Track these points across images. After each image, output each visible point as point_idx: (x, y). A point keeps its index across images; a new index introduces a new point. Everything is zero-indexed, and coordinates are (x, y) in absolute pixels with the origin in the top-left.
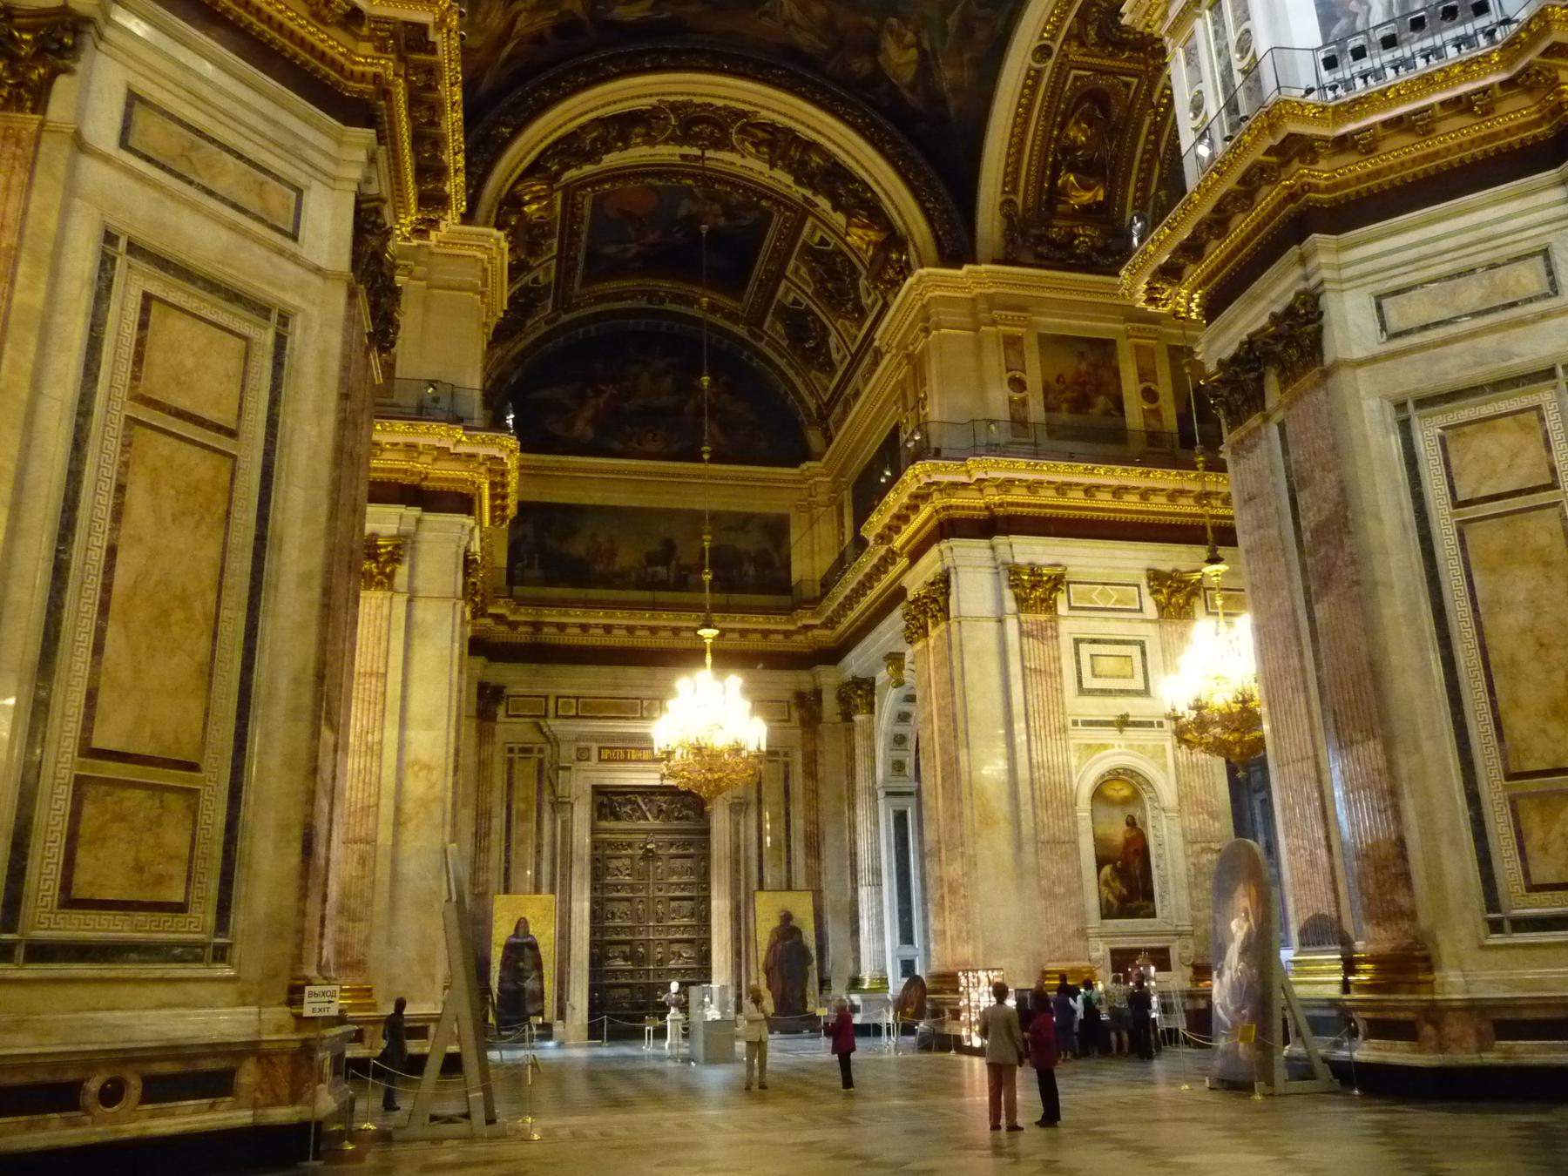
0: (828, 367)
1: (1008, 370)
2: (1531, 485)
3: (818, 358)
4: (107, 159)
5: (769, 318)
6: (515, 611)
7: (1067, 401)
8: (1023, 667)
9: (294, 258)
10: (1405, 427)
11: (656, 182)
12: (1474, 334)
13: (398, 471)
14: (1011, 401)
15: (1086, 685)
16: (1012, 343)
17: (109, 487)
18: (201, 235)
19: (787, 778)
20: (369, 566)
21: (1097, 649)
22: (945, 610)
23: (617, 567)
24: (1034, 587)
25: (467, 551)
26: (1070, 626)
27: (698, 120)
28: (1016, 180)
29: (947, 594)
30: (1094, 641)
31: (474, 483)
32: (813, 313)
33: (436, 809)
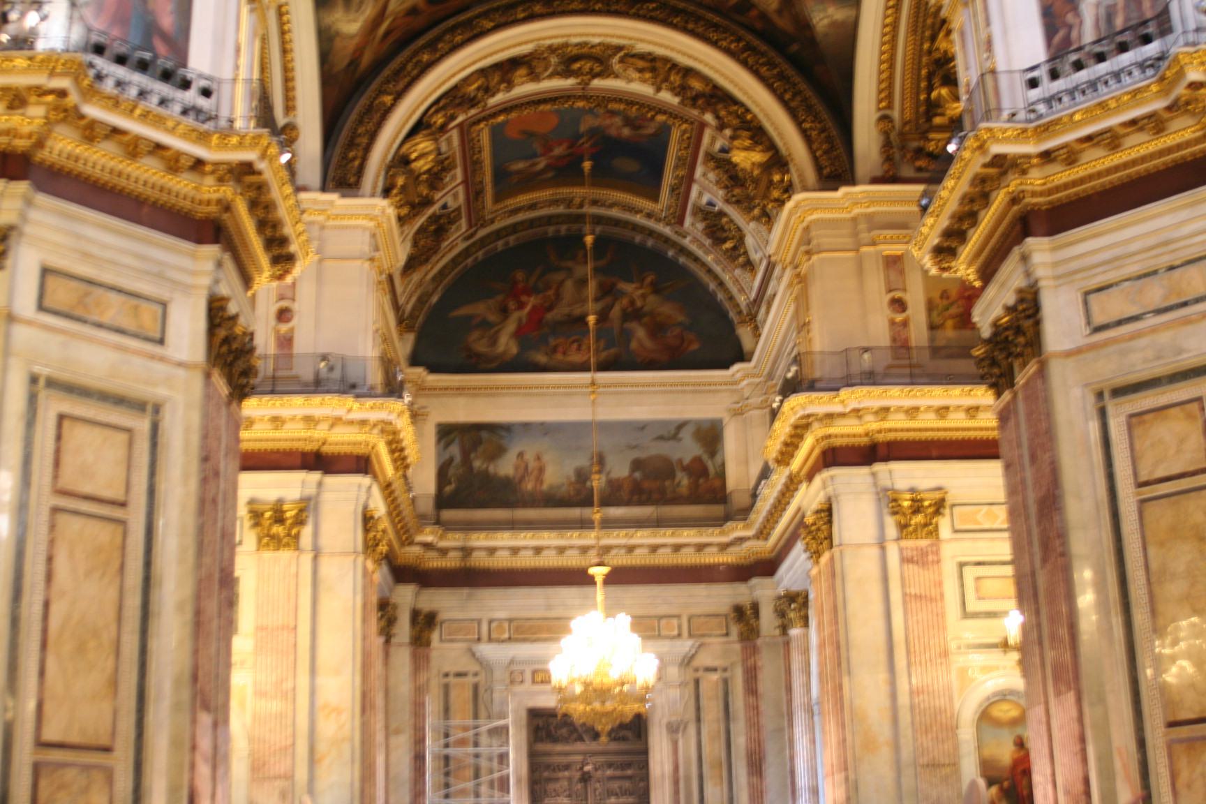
0: (749, 265)
2: (1192, 468)
3: (738, 255)
4: (29, 323)
6: (441, 538)
7: (953, 317)
8: (904, 595)
9: (162, 359)
10: (1103, 413)
11: (547, 107)
12: (1154, 330)
14: (892, 323)
17: (42, 559)
18: (95, 359)
19: (726, 694)
20: (278, 529)
22: (830, 537)
23: (545, 487)
24: (916, 511)
25: (365, 508)
27: (576, 58)
28: (890, 97)
29: (830, 522)
30: (979, 564)
33: (346, 748)
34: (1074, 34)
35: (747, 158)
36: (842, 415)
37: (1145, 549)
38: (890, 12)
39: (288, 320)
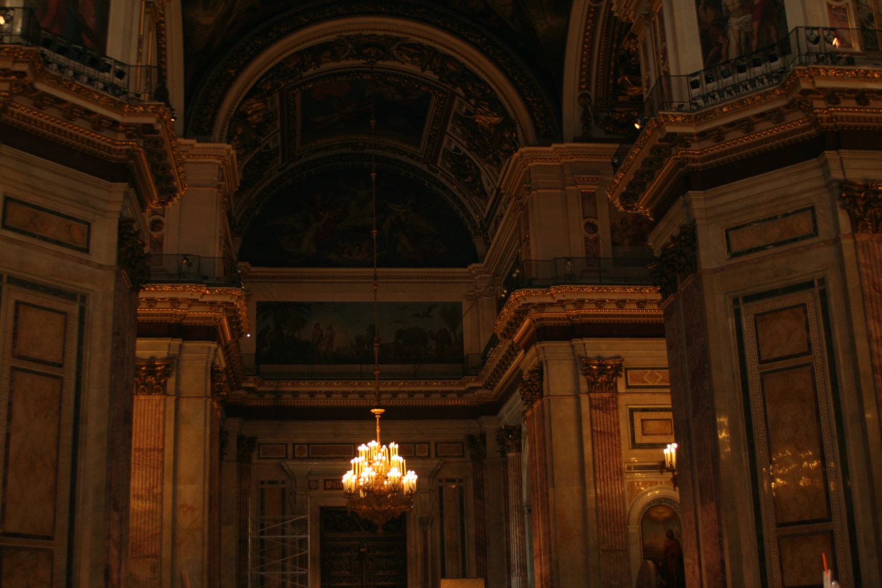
0: (483, 194)
1: (584, 219)
5: (440, 159)
8: (592, 431)
9: (88, 263)
13: (166, 315)
14: (586, 240)
15: (638, 441)
16: (588, 199)
18: (41, 261)
19: (462, 498)
21: (646, 415)
22: (541, 390)
25: (213, 363)
26: (626, 400)
29: (541, 380)
31: (215, 319)
32: (468, 158)
34: (723, 50)
35: (486, 120)
36: (551, 304)
37: (765, 406)
38: (590, 21)
39: (160, 229)
